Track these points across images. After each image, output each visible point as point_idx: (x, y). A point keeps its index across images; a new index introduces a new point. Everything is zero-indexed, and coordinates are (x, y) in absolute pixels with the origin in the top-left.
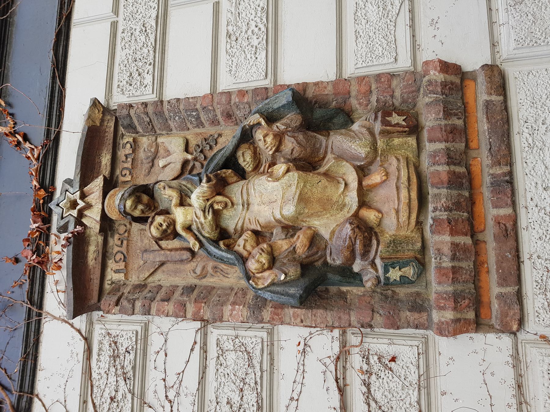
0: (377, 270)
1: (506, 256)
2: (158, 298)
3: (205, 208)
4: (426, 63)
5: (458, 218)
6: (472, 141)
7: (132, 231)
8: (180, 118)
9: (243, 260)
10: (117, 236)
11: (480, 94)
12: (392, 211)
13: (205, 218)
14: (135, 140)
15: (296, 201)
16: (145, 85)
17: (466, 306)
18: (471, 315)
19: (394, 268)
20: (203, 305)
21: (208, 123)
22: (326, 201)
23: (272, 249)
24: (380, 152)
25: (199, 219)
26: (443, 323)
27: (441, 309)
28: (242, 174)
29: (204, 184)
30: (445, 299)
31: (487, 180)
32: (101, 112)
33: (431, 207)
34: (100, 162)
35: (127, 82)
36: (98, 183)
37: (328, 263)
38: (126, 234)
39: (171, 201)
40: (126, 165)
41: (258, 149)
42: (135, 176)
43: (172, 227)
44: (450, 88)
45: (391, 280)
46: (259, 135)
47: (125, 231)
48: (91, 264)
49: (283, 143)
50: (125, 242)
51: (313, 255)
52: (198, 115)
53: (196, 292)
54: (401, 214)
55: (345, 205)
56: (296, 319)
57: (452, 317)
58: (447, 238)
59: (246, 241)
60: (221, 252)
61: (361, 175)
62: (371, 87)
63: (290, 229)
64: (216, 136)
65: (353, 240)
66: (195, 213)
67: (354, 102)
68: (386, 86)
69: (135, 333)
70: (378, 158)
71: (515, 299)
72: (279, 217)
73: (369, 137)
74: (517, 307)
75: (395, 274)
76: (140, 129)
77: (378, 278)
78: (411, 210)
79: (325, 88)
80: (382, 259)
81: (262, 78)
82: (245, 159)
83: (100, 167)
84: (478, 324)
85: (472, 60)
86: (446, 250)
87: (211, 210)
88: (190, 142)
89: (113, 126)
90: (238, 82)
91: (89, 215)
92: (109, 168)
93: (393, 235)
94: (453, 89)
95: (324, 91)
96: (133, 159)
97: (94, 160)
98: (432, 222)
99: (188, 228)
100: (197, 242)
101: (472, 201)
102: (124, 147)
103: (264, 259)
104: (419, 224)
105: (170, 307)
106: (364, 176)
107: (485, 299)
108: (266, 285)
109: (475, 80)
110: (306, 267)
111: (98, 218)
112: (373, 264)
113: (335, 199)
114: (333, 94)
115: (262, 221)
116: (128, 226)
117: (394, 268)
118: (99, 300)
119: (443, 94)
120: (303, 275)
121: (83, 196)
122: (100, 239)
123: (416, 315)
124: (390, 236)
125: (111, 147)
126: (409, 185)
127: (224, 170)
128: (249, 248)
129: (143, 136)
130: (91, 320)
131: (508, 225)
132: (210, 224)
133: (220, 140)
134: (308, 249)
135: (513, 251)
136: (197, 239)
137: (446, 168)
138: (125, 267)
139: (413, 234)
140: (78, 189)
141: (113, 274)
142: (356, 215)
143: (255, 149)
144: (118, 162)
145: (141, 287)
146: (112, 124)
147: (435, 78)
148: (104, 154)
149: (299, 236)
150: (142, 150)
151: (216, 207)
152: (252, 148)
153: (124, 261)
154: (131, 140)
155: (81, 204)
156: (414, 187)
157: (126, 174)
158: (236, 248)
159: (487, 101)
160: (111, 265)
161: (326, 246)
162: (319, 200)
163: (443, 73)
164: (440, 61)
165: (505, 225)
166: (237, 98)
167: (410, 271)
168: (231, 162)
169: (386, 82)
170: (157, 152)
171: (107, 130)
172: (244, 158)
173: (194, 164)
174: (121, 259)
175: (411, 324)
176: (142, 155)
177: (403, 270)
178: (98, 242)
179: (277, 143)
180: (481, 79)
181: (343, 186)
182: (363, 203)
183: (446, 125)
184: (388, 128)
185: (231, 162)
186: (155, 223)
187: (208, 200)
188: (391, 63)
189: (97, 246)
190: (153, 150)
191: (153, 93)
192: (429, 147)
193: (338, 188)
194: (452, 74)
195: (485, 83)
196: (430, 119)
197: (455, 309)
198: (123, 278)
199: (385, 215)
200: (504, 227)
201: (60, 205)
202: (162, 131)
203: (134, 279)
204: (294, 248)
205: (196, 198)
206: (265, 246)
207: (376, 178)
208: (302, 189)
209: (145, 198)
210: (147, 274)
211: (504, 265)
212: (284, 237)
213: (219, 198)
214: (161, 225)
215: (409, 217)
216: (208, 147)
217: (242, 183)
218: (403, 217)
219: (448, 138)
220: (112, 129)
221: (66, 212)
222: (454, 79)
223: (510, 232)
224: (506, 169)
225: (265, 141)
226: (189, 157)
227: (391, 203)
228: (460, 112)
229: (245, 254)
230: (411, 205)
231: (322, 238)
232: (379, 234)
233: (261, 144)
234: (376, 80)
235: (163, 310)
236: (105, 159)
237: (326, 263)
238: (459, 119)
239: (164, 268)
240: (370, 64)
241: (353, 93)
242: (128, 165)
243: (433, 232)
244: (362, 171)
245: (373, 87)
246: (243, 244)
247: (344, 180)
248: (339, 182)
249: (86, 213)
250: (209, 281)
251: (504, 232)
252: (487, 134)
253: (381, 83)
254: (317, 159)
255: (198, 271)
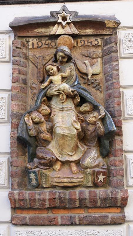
0: (34, 168)
1: (41, 220)
2: (20, 68)
3: (60, 91)
4: (127, 191)
5: (56, 202)
6: (92, 210)
7: (53, 49)
8: (109, 70)
9: (37, 109)
10: (50, 41)
11: (112, 214)
12: (58, 175)
13: (55, 91)
14: (99, 46)
15: (63, 133)
16: (128, 49)
17: (20, 204)
18: (17, 206)
19: (35, 176)
20: (18, 91)
21: (107, 85)
22: (64, 146)
23: (42, 123)
24: (86, 170)
25: (55, 88)
26: (14, 194)
27: (19, 194)
28: (78, 105)
29: (71, 89)
30: (23, 195)
31: (73, 215)
32: (113, 27)
33: (61, 191)
34: (87, 29)
35: (130, 39)
36: (75, 31)
37: (37, 147)
38: (51, 47)
39: (64, 73)
40: (86, 43)
41: (91, 113)
42: (81, 47)
43: (51, 74)
44: (114, 201)
45: (30, 174)
46: (96, 114)
47: (52, 46)
48: (36, 31)
49: (92, 125)
50: (47, 46)
51: (40, 141)
52: (110, 80)
53: (24, 85)
54: (57, 179)
55: (62, 155)
56: (13, 134)
57: (16, 198)
58: (47, 197)
59: (46, 110)
60: (40, 99)
61: (76, 162)
62: (118, 166)
63: (51, 130)
64: (100, 90)
65: (46, 159)
66: (57, 86)
67: (112, 158)
68: (117, 173)
69: (5, 57)
70: (83, 170)
71: (24, 223)
72: (56, 126)
73: (92, 165)
74: (21, 223)
75: (32, 176)
76: (105, 48)
77: (31, 169)
78: (59, 183)
79: (119, 145)
80: (39, 171)
81: (128, 113)
82: (85, 107)
83: (85, 29)
84: (14, 209)
85: (130, 212)
86: (42, 197)
87: (59, 93)
88: (98, 76)
89: (107, 33)
90: (127, 100)
91: (59, 28)
92: (84, 34)
93: (49, 176)
94: (114, 202)
95: (117, 144)
96: (89, 46)
97: (88, 26)
98: (54, 191)
99: (51, 82)
100: (44, 87)
101: (64, 208)
102: (96, 40)
103: (36, 120)
104: (54, 187)
105: (16, 75)
106: (76, 163)
107: (24, 212)
108: (26, 121)
109: (121, 212)
110: (36, 138)
111: (57, 33)
112: (37, 167)
113: (65, 150)
114: (116, 149)
115: (54, 117)
116: (55, 47)
117: (35, 176)
118: (19, 37)
119: (111, 198)
120: (31, 137)
121: (68, 24)
122: (47, 34)
123: (16, 184)
124: (48, 174)
125: (96, 33)
126: (70, 183)
127: (79, 98)
128: (43, 112)
129: (102, 50)
130: (10, 32)
131: (54, 222)
132: (52, 93)
133: (98, 92)
134: (42, 139)
135: (43, 223)
136: (46, 87)
137: (77, 198)
138: (35, 48)
139: (49, 184)
140: (72, 21)
141: (32, 42)
142: (57, 160)
143: (91, 112)
144: (88, 38)
145: (27, 58)
146: (108, 33)
147: (119, 194)
148: (91, 30)
149: (48, 135)
150: (94, 50)
151: (61, 95)
152: (91, 110)
153: (38, 47)
154: (100, 44)
155: (64, 23)
156: (69, 185)
157: (81, 43)
158: (43, 105)
159: (108, 216)
160: (35, 41)
161: (44, 147)
162: (64, 144)
163: (122, 198)
164: (127, 197)
165: (54, 221)
166: (117, 101)
167: (34, 182)
168: (83, 100)
169: (119, 173)
170: (93, 58)
171: (104, 30)
172: (86, 106)
173: (86, 79)
174: (39, 45)
175: (13, 182)
176: (92, 50)
177: (34, 179)
178: (46, 33)
179: (92, 123)
180: (120, 215)
181: (70, 154)
182: (64, 163)
183: (97, 198)
184: (96, 174)
185: (83, 100)
186: (52, 67)
187: (64, 92)
188: (131, 176)
189: (45, 33)
190: (94, 56)
191: (124, 54)
192: (87, 191)
193: (70, 152)
194: (121, 202)
195: (116, 216)
196: (100, 192)
197: (19, 199)
198: (29, 48)
199: (58, 172)
200: (53, 220)
201: (64, 12)
202: (105, 60)
203: (30, 53)
204: (43, 133)
205: (66, 86)
206: (43, 119)
207: (74, 168)
208: (68, 136)
209: (65, 60)
210: (32, 60)
211: (38, 220)
212: (48, 128)
213: (65, 97)
214: (52, 70)
215: (56, 182)
216: (94, 86)
217: (73, 106)
218: (56, 180)
219: (91, 199)
220: (105, 33)
221: (60, 15)
222: (123, 203)
223: (51, 223)
224: (78, 223)
225: (93, 117)
226: (89, 77)
227: (62, 175)
228: (104, 205)
229: (40, 110)
230: (61, 183)
231: (48, 145)
232: (49, 170)
233: (92, 115)
234: (121, 169)
235: (15, 71)
236: (89, 31)
237: (37, 146)
238: (100, 204)
239: (35, 68)
240: (131, 166)
241: (115, 158)
242: (86, 44)
243: (50, 191)
244: (78, 163)
245: (117, 167)
246: (45, 109)
247: (74, 154)
248: (72, 152)
249: (60, 26)
250: (29, 91)
251: (51, 220)
252: (94, 216)
253: (119, 171)
254: (85, 141)
255: (34, 86)
